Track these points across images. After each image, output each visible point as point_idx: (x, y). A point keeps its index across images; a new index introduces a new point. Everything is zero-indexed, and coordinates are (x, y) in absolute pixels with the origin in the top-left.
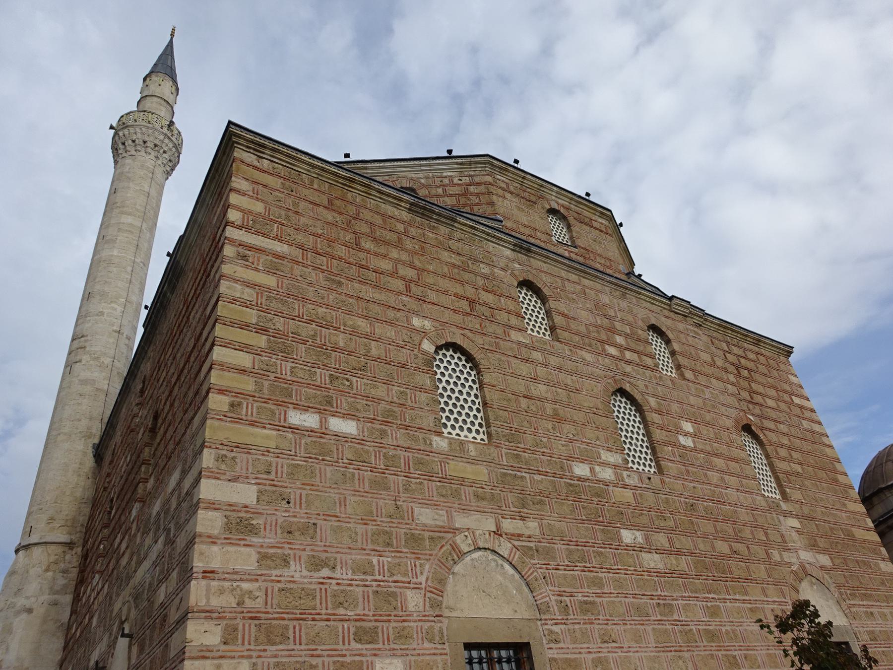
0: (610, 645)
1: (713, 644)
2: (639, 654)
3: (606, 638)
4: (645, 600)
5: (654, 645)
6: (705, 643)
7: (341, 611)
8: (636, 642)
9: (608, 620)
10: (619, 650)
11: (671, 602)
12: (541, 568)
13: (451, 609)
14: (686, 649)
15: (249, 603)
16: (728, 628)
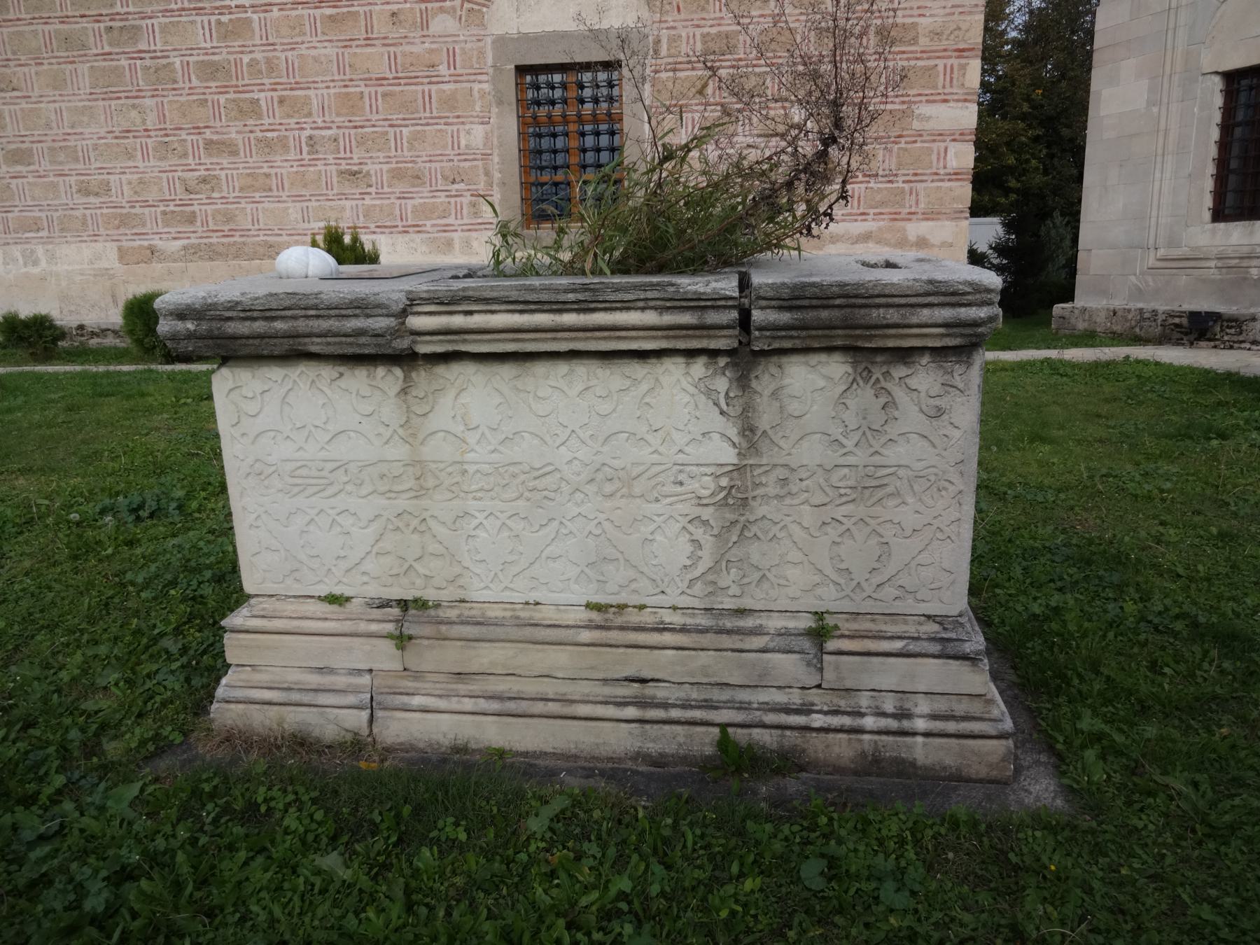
0: (8, 95)
1: (213, 84)
2: (57, 105)
4: (84, 24)
5: (88, 91)
6: (195, 82)
8: (55, 88)
9: (8, 60)
10: (23, 101)
11: (137, 23)
14: (149, 94)
16: (258, 56)
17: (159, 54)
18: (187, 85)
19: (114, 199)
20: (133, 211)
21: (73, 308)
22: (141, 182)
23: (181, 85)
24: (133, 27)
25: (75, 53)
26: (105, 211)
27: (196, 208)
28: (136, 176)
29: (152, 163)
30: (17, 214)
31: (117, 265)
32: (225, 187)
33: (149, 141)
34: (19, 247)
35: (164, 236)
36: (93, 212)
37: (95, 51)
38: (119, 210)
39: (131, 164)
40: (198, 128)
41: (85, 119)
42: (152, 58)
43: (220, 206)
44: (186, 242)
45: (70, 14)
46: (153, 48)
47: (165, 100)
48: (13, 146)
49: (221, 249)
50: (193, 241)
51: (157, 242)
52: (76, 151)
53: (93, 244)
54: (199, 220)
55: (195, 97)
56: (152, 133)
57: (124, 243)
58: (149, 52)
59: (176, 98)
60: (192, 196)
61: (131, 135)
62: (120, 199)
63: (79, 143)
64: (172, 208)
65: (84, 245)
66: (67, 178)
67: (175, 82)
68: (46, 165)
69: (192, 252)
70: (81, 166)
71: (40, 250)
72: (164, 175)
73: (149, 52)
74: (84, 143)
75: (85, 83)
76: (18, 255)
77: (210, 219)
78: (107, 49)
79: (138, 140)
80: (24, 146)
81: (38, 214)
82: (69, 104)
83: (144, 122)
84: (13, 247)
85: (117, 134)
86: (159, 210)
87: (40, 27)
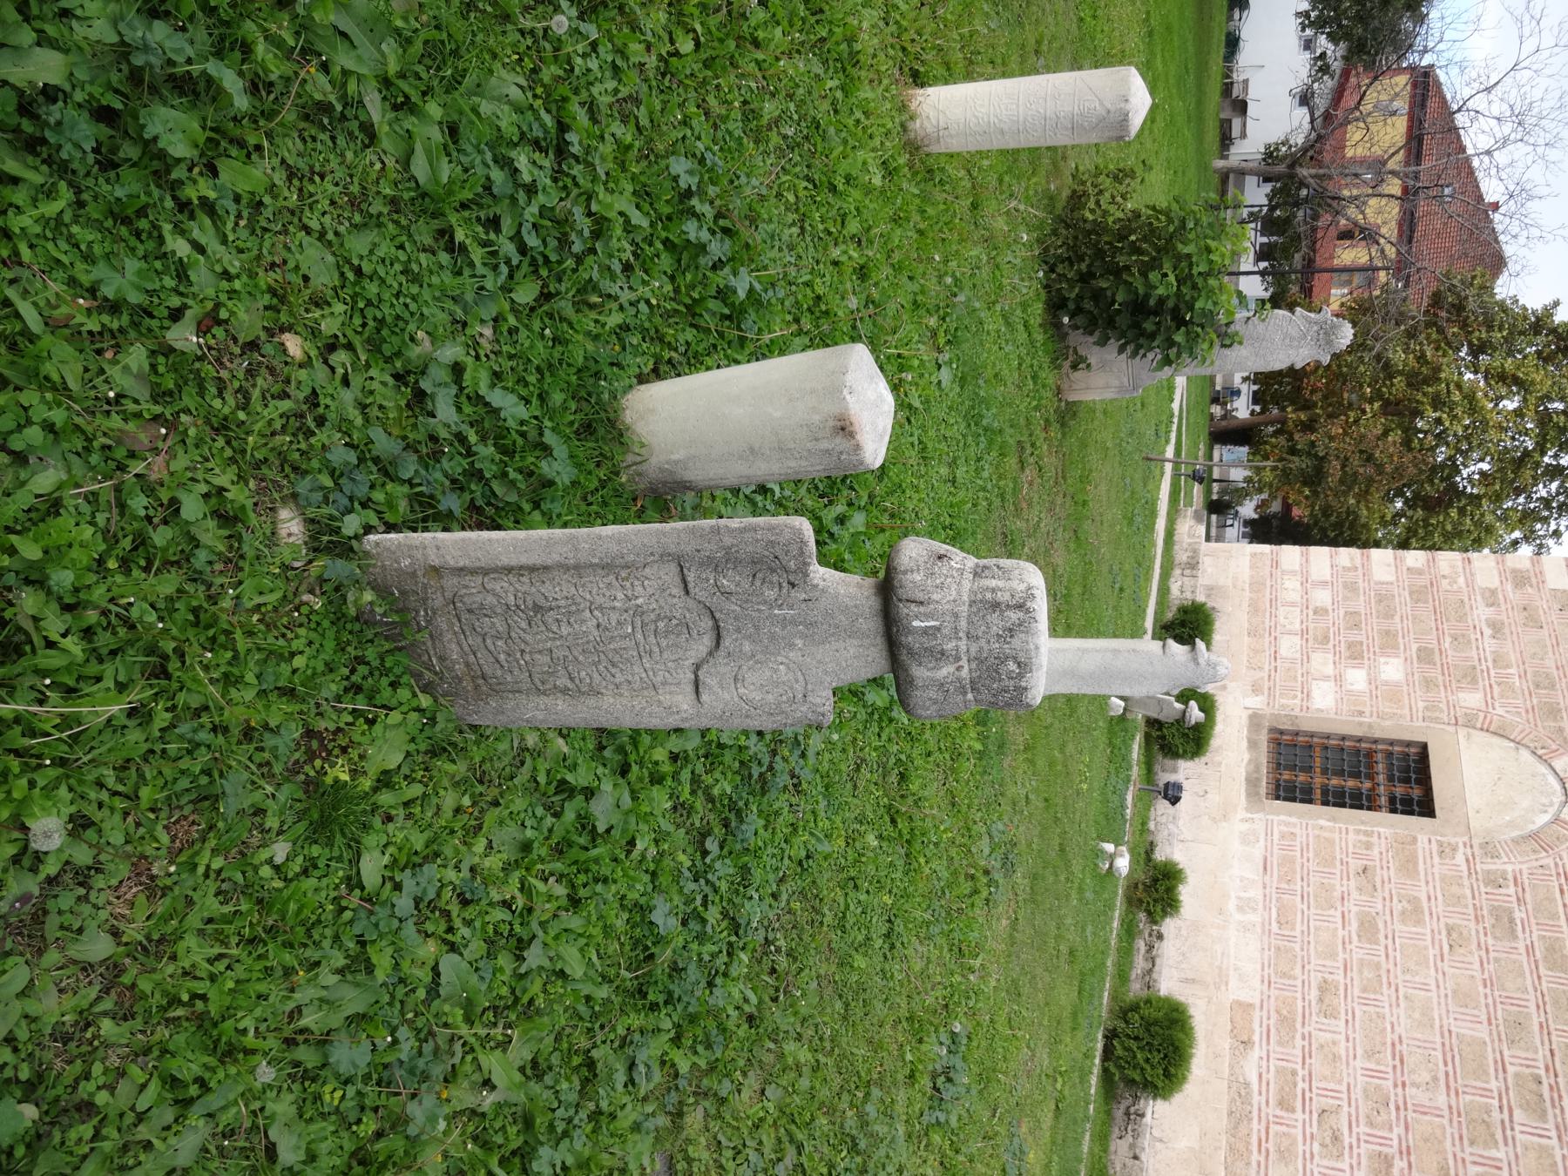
2: (1433, 987)
3: (1455, 935)
7: (1448, 640)
8: (1454, 992)
10: (1437, 952)
12: (1556, 865)
13: (1469, 736)
14: (1454, 1104)
15: (1445, 583)
17: (1509, 1133)
18: (1469, 1159)
19: (1314, 1018)
20: (1298, 1036)
21: (1184, 932)
22: (1336, 1057)
23: (1468, 1150)
24: (1544, 1111)
25: (1501, 1028)
26: (1300, 1003)
27: (1299, 1115)
28: (1343, 1053)
29: (1360, 1078)
30: (1300, 906)
31: (1232, 997)
32: (1325, 1162)
33: (1390, 1083)
34: (1261, 898)
35: (1264, 1063)
36: (1299, 989)
37: (1506, 1053)
38: (1299, 1019)
39: (1359, 1052)
40: (1409, 1153)
41: (1417, 1015)
42: (1503, 1122)
43: (1301, 1148)
44: (1255, 1087)
45: (1554, 1038)
46: (1518, 1128)
47: (1445, 1122)
48: (1381, 926)
49: (1243, 1130)
50: (1256, 1099)
51: (1256, 1053)
52: (1375, 992)
53: (1258, 977)
54: (1285, 1114)
55: (1451, 1162)
56: (1400, 1090)
57: (1257, 1014)
58: (1511, 1121)
59: (1448, 1136)
60: (1315, 1116)
61: (1397, 1062)
62: (1314, 1025)
63: (1385, 998)
64: (1300, 1085)
65: (1259, 967)
66: (1341, 972)
67: (1472, 1143)
68: (1358, 954)
69: (1241, 1092)
70: (1357, 992)
71: (1255, 918)
72: (1344, 1089)
73: (1511, 1121)
74: (1387, 1005)
75: (1464, 1029)
76: (1251, 894)
77: (1284, 1129)
78: (1511, 1069)
79: (1390, 1070)
80: (1381, 936)
81: (1298, 927)
82: (1435, 1000)
83: (1414, 1084)
84: (1260, 892)
85: (1398, 1047)
86: (1299, 1068)
87: (1532, 998)
